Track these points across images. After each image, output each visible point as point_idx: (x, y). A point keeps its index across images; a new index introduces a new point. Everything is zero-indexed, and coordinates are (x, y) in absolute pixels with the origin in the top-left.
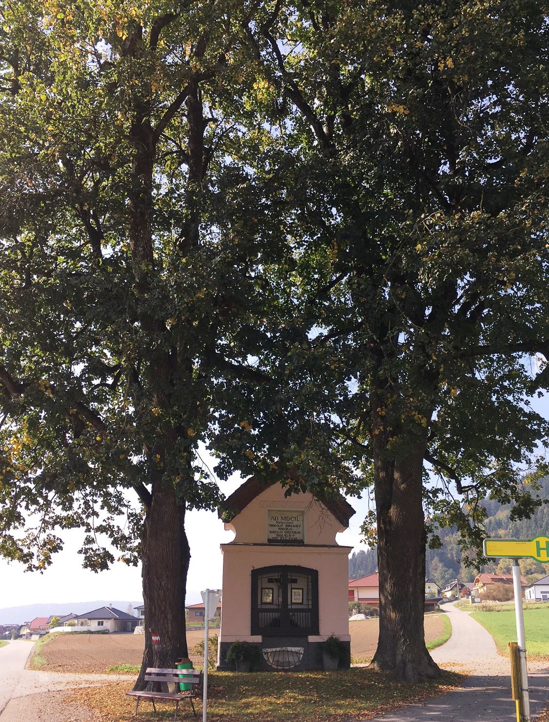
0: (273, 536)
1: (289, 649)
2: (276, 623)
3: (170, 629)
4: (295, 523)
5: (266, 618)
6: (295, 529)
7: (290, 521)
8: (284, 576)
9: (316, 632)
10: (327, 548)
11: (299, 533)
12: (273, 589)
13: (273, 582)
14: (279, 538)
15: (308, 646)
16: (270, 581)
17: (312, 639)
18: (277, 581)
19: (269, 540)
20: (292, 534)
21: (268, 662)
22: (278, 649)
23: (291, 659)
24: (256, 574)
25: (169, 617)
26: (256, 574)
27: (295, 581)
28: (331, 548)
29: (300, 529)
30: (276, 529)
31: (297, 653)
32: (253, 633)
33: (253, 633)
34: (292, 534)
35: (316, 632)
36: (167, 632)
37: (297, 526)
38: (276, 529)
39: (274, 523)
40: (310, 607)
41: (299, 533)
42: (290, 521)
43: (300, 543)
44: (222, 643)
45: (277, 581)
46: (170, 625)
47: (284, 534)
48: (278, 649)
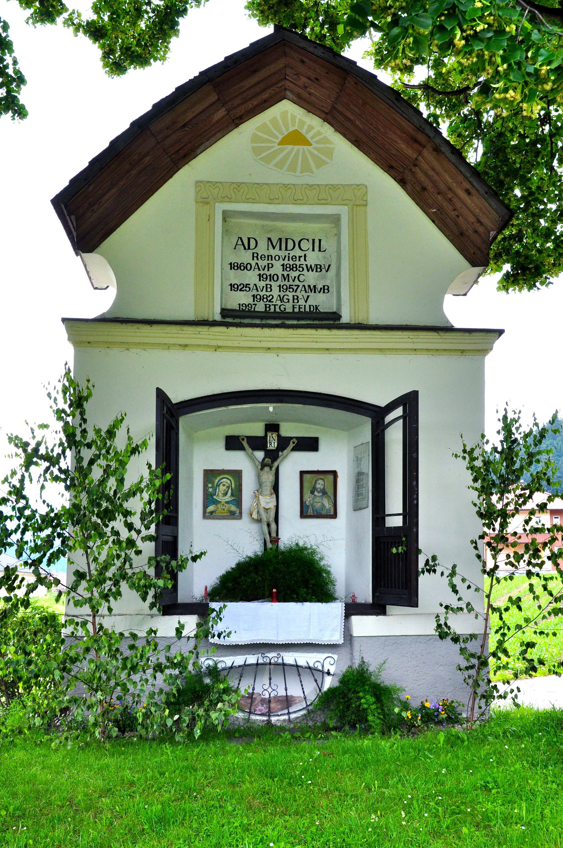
0: (242, 299)
4: (313, 258)
6: (311, 278)
7: (297, 252)
11: (325, 289)
13: (242, 448)
14: (260, 307)
16: (233, 443)
19: (225, 312)
20: (301, 294)
23: (295, 691)
27: (310, 445)
29: (329, 279)
30: (251, 277)
34: (301, 294)
37: (318, 268)
38: (251, 277)
39: (245, 257)
41: (325, 289)
42: (297, 252)
43: (330, 320)
47: (275, 292)
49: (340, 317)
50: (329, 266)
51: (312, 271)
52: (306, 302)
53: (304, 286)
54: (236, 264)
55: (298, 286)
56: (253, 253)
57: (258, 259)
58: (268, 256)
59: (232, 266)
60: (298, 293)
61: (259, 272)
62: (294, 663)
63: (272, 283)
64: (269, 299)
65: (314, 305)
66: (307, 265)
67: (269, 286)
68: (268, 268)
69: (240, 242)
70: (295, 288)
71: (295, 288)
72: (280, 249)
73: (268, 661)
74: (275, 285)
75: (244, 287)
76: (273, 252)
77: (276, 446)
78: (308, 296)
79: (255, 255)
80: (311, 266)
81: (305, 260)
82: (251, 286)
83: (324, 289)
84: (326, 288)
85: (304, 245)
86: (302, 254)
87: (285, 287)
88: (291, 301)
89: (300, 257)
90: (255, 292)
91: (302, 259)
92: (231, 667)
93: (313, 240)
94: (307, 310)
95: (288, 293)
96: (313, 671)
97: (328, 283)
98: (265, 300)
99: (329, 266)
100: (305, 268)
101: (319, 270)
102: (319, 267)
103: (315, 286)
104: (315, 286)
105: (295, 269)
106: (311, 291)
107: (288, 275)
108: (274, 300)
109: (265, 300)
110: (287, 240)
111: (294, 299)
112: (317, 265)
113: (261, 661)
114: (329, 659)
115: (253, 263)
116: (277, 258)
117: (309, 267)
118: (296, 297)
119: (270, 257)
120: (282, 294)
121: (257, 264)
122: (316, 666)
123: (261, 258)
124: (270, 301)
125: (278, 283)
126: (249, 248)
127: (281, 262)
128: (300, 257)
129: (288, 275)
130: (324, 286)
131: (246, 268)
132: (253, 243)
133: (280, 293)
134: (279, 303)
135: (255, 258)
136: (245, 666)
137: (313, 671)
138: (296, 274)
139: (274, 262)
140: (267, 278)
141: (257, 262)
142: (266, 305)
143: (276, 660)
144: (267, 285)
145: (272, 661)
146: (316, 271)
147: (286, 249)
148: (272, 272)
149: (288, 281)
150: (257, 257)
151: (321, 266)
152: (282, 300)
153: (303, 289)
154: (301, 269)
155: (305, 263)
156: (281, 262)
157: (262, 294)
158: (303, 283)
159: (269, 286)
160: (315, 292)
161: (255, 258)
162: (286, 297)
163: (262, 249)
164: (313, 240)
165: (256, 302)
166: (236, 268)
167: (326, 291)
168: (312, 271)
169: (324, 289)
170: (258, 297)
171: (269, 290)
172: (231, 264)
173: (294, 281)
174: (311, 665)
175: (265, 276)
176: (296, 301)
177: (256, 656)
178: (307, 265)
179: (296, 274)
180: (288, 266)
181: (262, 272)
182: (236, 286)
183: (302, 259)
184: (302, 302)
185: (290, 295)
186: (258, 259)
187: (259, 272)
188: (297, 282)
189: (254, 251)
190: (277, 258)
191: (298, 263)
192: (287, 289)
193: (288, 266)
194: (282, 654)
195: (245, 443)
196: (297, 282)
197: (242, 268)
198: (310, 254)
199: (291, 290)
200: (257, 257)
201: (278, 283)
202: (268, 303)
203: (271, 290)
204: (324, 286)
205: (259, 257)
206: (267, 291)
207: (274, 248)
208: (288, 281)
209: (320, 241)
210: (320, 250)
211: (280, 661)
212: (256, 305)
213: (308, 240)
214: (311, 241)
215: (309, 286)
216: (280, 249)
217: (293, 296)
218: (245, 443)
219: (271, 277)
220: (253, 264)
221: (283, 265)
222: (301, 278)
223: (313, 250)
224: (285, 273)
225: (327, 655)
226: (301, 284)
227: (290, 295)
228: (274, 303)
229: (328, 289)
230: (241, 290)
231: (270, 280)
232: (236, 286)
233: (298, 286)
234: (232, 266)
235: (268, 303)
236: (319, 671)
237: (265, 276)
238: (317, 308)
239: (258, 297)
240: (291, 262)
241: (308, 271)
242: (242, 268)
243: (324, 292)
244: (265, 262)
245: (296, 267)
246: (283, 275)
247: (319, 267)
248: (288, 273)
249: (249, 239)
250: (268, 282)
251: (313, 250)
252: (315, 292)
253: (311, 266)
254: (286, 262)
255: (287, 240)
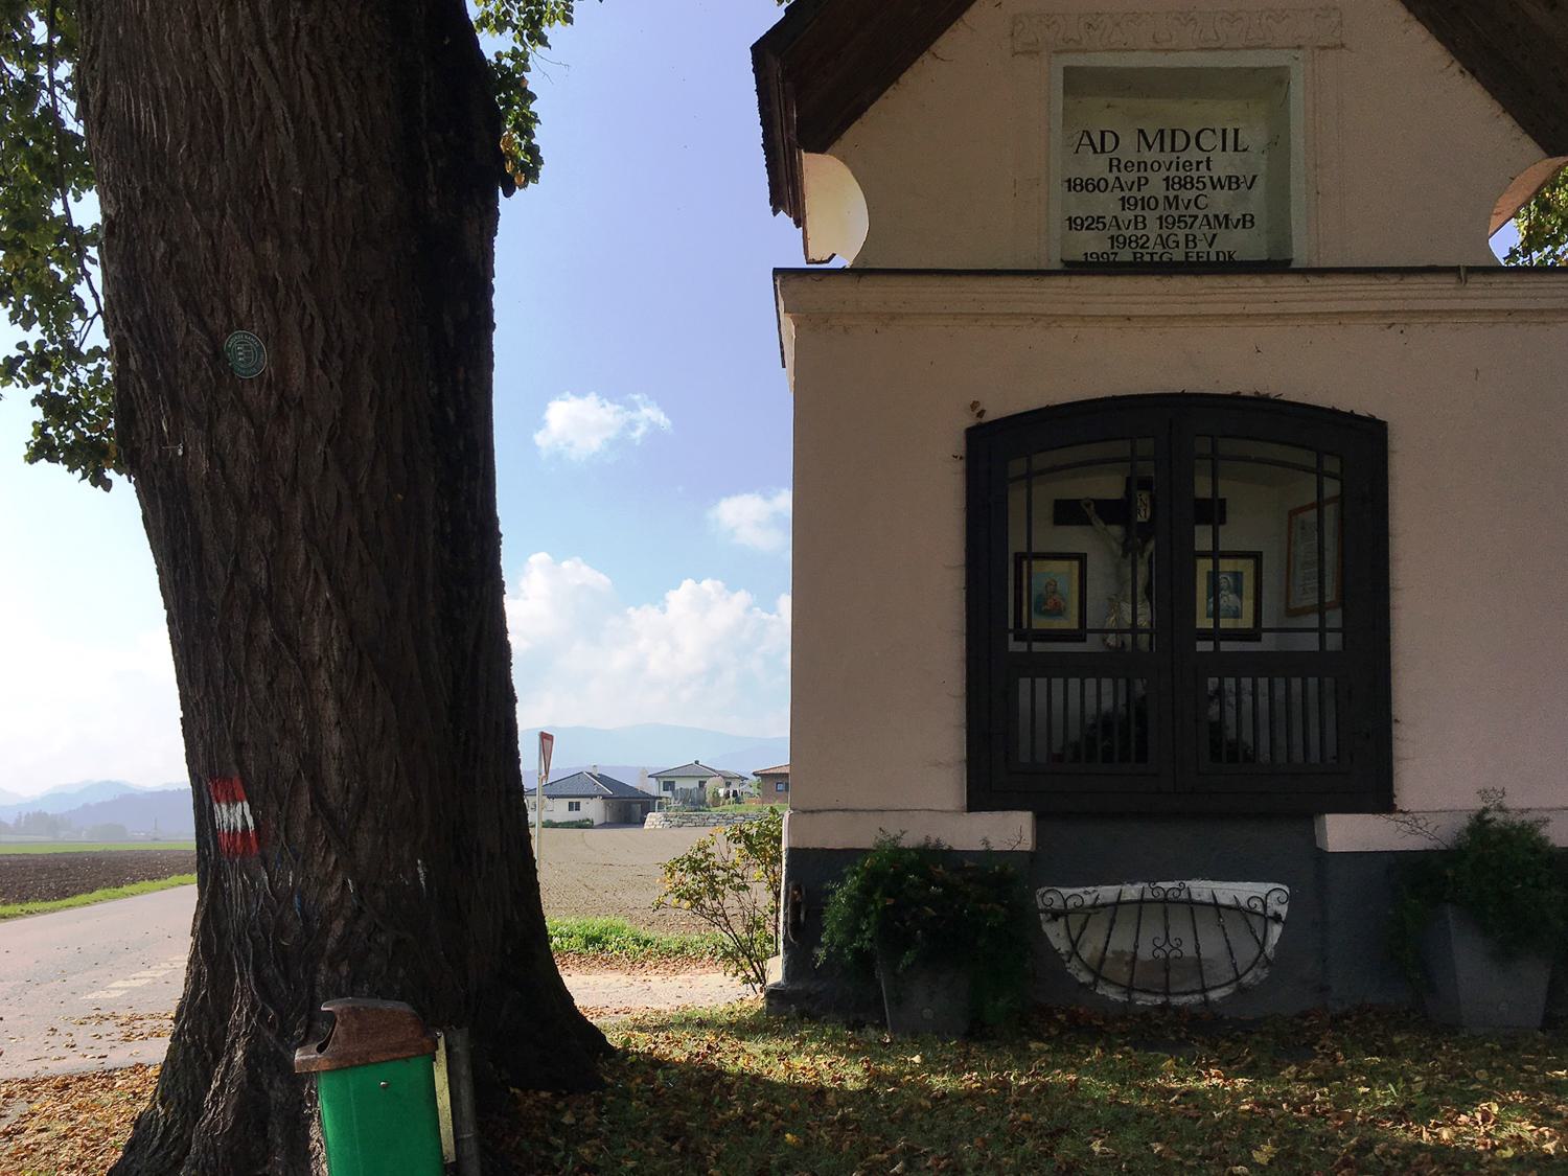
0: (1091, 244)
1: (1201, 889)
2: (1117, 740)
3: (334, 740)
5: (1062, 705)
6: (1219, 201)
7: (1193, 154)
8: (1160, 459)
9: (1379, 797)
10: (1449, 281)
11: (1247, 221)
12: (1081, 559)
13: (1085, 521)
14: (1126, 255)
15: (1316, 873)
16: (1068, 513)
17: (1344, 832)
18: (1113, 512)
20: (1201, 231)
21: (1073, 967)
22: (1132, 892)
23: (1212, 946)
24: (999, 453)
25: (321, 638)
26: (999, 453)
28: (1476, 281)
29: (1255, 201)
30: (1106, 204)
31: (1236, 908)
32: (983, 795)
33: (983, 795)
34: (1201, 231)
35: (1379, 797)
36: (311, 764)
37: (1233, 182)
38: (1106, 204)
39: (1096, 167)
40: (1334, 642)
41: (1247, 221)
42: (1193, 154)
43: (1276, 266)
44: (792, 851)
45: (1113, 512)
46: (330, 711)
47: (1153, 230)
48: (1132, 892)
49: (1289, 261)
50: (1254, 177)
51: (1222, 188)
52: (1210, 246)
53: (1206, 216)
54: (1078, 182)
55: (1196, 217)
56: (1111, 160)
57: (1119, 171)
58: (1139, 163)
59: (1071, 185)
60: (1195, 230)
61: (1123, 194)
62: (1233, 903)
63: (1146, 213)
64: (1141, 242)
65: (1226, 250)
66: (1211, 178)
67: (1140, 219)
68: (1139, 185)
69: (1086, 140)
70: (1189, 221)
71: (1189, 221)
72: (1162, 150)
73: (1162, 896)
74: (1152, 217)
75: (1095, 223)
76: (1149, 156)
77: (1148, 514)
78: (1215, 236)
79: (1115, 163)
80: (1219, 179)
81: (1209, 169)
82: (1107, 221)
83: (1244, 221)
84: (1248, 218)
85: (1207, 141)
86: (1203, 157)
87: (1170, 220)
88: (1182, 244)
89: (1198, 163)
90: (1114, 231)
91: (1203, 167)
92: (1093, 906)
93: (1224, 131)
94: (1213, 258)
95: (1176, 230)
96: (1222, 910)
97: (1252, 209)
98: (1133, 245)
99: (1254, 177)
100: (1209, 184)
101: (1234, 186)
102: (1234, 180)
103: (1226, 216)
104: (1226, 216)
105: (1189, 186)
106: (1220, 226)
107: (1176, 197)
108: (1150, 244)
109: (1133, 245)
110: (1173, 132)
111: (1187, 241)
112: (1230, 177)
113: (1148, 896)
114: (1275, 895)
115: (1111, 178)
116: (1156, 166)
117: (1215, 180)
118: (1191, 238)
119: (1142, 165)
120: (1165, 233)
121: (1118, 178)
122: (1252, 904)
123: (1126, 167)
124: (1142, 247)
125: (1157, 213)
126: (1103, 151)
127: (1164, 173)
128: (1198, 163)
129: (1176, 197)
130: (1244, 216)
131: (1097, 187)
132: (1110, 140)
133: (1161, 232)
134: (1159, 249)
135: (1115, 169)
136: (1118, 903)
137: (1222, 910)
138: (1193, 194)
139: (1149, 174)
140: (1136, 204)
141: (1118, 174)
142: (1135, 254)
143: (1177, 893)
144: (1136, 217)
145: (1170, 896)
146: (1230, 188)
147: (1173, 150)
148: (1146, 192)
149: (1177, 208)
150: (1118, 166)
151: (1238, 178)
152: (1165, 244)
153: (1205, 222)
154: (1201, 186)
155: (1208, 173)
156: (1164, 173)
157: (1127, 234)
158: (1205, 212)
159: (1140, 219)
160: (1227, 227)
161: (1115, 169)
162: (1172, 238)
163: (1128, 150)
164: (1224, 131)
165: (1116, 250)
166: (1078, 188)
167: (1248, 224)
168: (1222, 188)
169: (1244, 221)
170: (1121, 239)
171: (1140, 225)
172: (1069, 180)
173: (1186, 208)
174: (1243, 903)
175: (1132, 201)
176: (1191, 244)
177: (1139, 886)
178: (1211, 178)
179: (1193, 194)
180: (1176, 180)
181: (1127, 194)
182: (1079, 221)
183: (1203, 167)
184: (1202, 246)
185: (1181, 234)
186: (1119, 171)
187: (1123, 194)
188: (1193, 210)
189: (1113, 155)
190: (1156, 166)
191: (1195, 174)
192: (1174, 224)
193: (1176, 180)
194: (1187, 883)
195: (1091, 511)
196: (1193, 210)
197: (1090, 187)
198: (1218, 158)
199: (1182, 225)
200: (1118, 166)
201: (1157, 213)
202: (1138, 250)
203: (1145, 227)
204: (1244, 216)
205: (1122, 166)
206: (1136, 228)
207: (1150, 147)
208: (1177, 208)
209: (1236, 131)
210: (1236, 150)
211: (1184, 896)
212: (1116, 254)
213: (1213, 131)
214: (1220, 134)
215: (1216, 217)
216: (1162, 150)
217: (1187, 236)
218: (1091, 511)
219: (1145, 203)
220: (1111, 178)
221: (1167, 179)
222: (1202, 201)
223: (1224, 149)
224: (1171, 194)
225: (1271, 886)
226: (1201, 214)
227: (1181, 234)
228: (1149, 251)
229: (1252, 221)
230: (1087, 228)
231: (1143, 209)
232: (1079, 221)
233: (1196, 217)
234: (1071, 185)
235: (1138, 250)
236: (1258, 914)
237: (1132, 201)
238: (1230, 257)
239: (1121, 239)
240: (1182, 173)
241: (1214, 188)
242: (1090, 187)
243: (1244, 227)
244: (1133, 176)
245: (1191, 182)
246: (1167, 198)
247: (1234, 180)
248: (1175, 193)
249: (1103, 133)
250: (1138, 211)
251: (1224, 149)
252: (1227, 227)
253: (1219, 179)
254: (1173, 173)
255: (1173, 132)
